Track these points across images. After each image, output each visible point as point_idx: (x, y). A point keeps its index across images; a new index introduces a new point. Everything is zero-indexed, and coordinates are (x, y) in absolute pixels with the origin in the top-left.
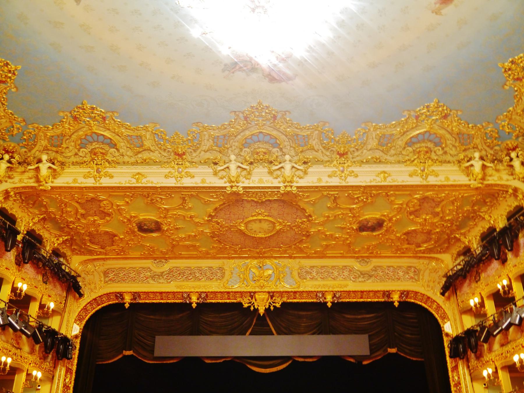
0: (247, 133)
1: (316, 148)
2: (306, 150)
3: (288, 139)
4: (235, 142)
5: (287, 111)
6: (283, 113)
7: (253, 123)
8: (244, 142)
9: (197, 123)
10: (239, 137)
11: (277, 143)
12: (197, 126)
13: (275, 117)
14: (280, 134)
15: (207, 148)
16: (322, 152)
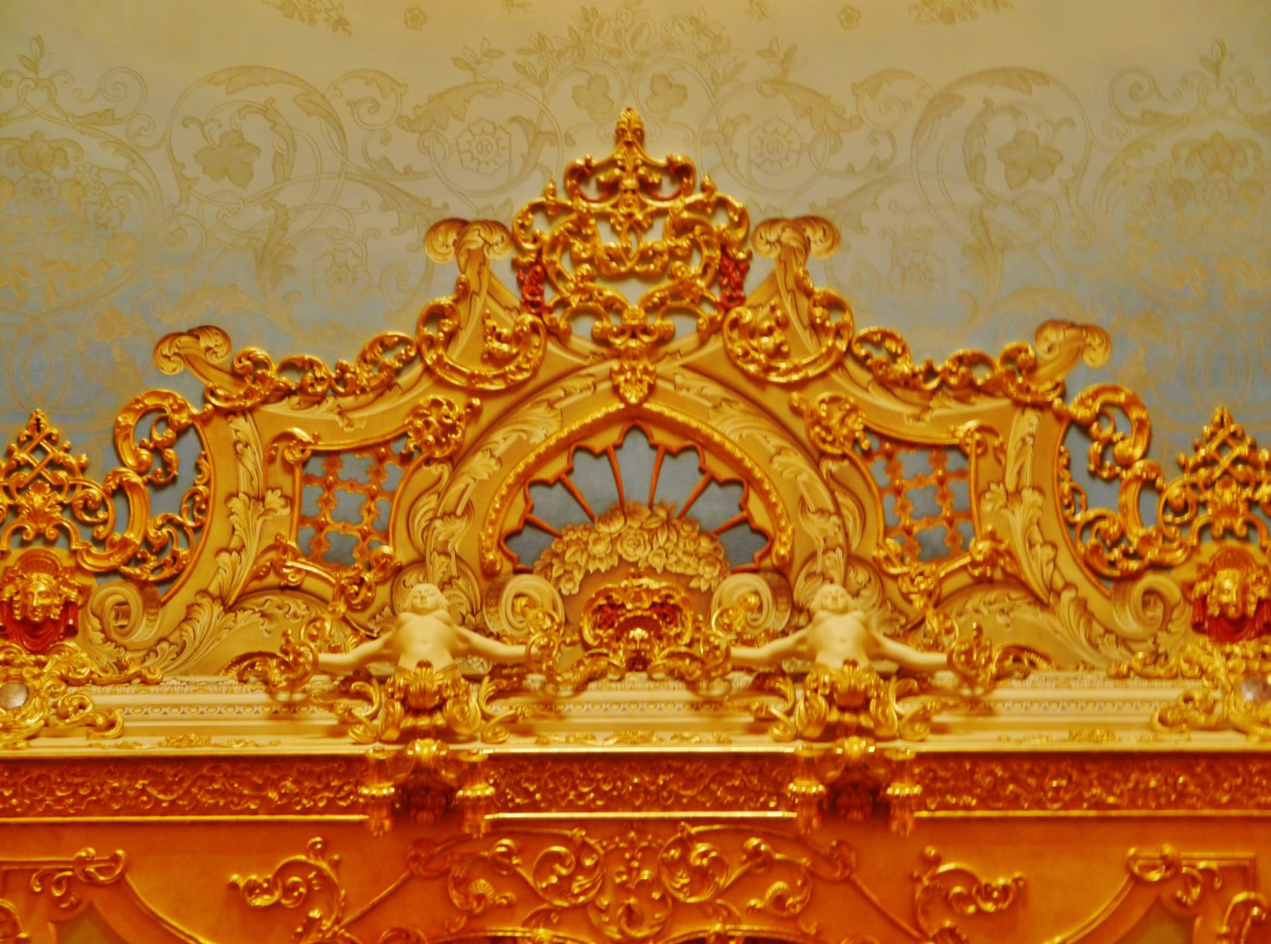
0: (541, 427)
1: (1034, 568)
2: (963, 591)
3: (832, 482)
4: (450, 514)
5: (813, 220)
6: (788, 236)
7: (582, 332)
8: (513, 521)
9: (194, 333)
10: (480, 466)
11: (747, 521)
12: (187, 359)
13: (730, 272)
14: (774, 441)
15: (244, 573)
16: (1082, 605)
